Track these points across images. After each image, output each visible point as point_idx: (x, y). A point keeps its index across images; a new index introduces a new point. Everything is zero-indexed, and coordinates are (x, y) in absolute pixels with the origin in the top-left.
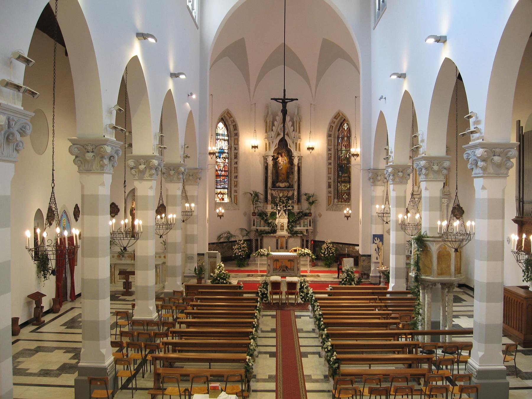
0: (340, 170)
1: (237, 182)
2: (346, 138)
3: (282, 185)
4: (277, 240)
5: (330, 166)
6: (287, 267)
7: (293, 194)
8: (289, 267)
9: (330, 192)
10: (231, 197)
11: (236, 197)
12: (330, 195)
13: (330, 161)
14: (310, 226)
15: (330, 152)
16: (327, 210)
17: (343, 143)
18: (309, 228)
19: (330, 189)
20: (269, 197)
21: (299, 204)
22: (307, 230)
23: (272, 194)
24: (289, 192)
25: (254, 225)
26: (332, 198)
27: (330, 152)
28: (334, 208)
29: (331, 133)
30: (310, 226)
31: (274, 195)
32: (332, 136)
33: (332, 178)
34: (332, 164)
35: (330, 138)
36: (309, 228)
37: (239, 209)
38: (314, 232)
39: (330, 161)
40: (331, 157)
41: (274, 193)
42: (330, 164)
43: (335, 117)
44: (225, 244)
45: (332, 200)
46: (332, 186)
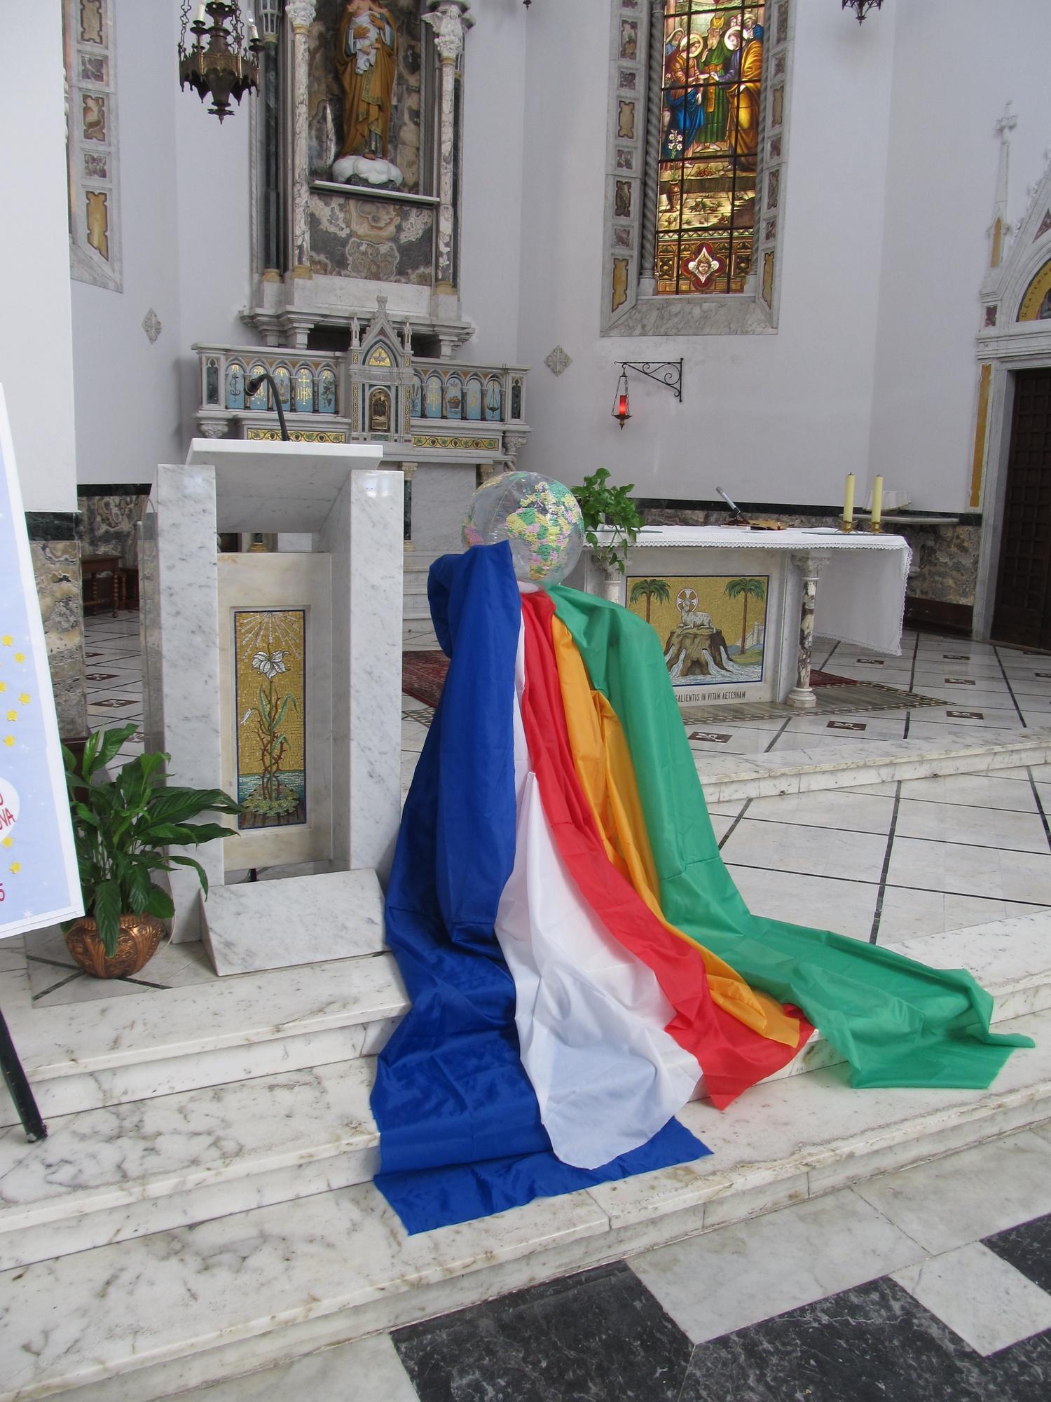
0: (673, 124)
1: (100, 101)
3: (376, 170)
6: (716, 640)
12: (622, 251)
14: (516, 414)
16: (605, 333)
19: (623, 220)
20: (300, 232)
24: (405, 217)
25: (213, 396)
26: (633, 267)
31: (325, 224)
33: (637, 161)
34: (640, 82)
37: (119, 290)
40: (632, 41)
41: (323, 210)
42: (628, 79)
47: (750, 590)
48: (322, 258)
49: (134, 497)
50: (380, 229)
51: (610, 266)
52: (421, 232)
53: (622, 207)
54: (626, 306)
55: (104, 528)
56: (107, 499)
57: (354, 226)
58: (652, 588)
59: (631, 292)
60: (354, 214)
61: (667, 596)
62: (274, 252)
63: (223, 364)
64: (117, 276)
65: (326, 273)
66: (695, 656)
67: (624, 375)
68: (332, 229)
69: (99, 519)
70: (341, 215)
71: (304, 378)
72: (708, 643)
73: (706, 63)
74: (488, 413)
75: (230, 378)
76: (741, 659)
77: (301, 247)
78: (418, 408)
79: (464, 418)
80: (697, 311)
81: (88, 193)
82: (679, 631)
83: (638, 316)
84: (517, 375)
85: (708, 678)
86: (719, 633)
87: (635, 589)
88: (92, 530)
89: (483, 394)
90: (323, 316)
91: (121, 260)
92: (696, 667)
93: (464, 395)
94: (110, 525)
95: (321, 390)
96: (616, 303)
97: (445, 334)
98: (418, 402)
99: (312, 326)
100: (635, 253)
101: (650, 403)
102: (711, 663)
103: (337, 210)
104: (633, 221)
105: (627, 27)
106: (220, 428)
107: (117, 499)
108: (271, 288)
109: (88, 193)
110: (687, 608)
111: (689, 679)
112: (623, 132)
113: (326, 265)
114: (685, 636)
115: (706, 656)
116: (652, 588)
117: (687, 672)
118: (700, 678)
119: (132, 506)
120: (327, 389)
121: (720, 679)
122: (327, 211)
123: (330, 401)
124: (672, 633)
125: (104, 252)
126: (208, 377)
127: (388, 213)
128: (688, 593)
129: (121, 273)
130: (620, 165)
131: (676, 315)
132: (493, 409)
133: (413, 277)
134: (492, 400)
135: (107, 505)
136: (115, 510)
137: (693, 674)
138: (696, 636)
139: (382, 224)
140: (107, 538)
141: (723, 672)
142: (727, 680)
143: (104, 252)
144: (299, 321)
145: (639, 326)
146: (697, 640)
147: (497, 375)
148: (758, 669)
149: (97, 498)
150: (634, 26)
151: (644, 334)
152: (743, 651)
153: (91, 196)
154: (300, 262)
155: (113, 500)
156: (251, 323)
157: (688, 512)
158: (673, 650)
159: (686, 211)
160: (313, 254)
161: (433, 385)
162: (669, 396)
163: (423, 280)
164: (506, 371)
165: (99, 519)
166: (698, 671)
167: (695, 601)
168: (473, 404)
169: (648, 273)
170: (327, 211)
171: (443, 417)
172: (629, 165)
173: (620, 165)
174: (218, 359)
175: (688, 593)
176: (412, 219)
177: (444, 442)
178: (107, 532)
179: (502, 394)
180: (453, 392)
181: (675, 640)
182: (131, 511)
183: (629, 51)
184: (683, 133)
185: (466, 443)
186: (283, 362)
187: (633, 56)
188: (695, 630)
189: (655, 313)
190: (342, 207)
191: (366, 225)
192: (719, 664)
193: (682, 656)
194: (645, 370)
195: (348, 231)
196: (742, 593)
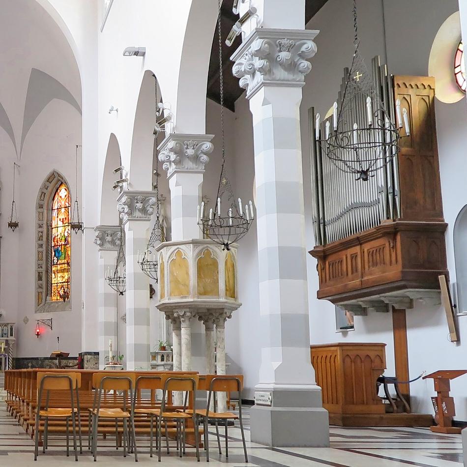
2: (63, 210)
5: (40, 249)
9: (40, 287)
12: (40, 290)
13: (40, 242)
14: (11, 335)
15: (40, 230)
17: (59, 217)
18: (10, 338)
19: (40, 282)
22: (7, 341)
26: (44, 294)
27: (40, 230)
29: (42, 202)
30: (11, 335)
32: (45, 207)
33: (44, 267)
34: (44, 247)
35: (40, 210)
36: (10, 338)
38: (17, 344)
39: (40, 242)
40: (42, 236)
42: (41, 246)
43: (49, 180)
46: (44, 278)
53: (40, 278)
54: (41, 305)
73: (61, 240)
74: (4, 335)
80: (57, 305)
84: (12, 325)
100: (44, 291)
101: (46, 330)
104: (44, 282)
105: (40, 233)
112: (39, 259)
130: (39, 268)
132: (5, 334)
147: (6, 325)
150: (42, 232)
159: (58, 278)
162: (49, 328)
169: (49, 295)
172: (41, 267)
173: (39, 268)
183: (41, 239)
184: (57, 257)
187: (42, 240)
194: (43, 322)
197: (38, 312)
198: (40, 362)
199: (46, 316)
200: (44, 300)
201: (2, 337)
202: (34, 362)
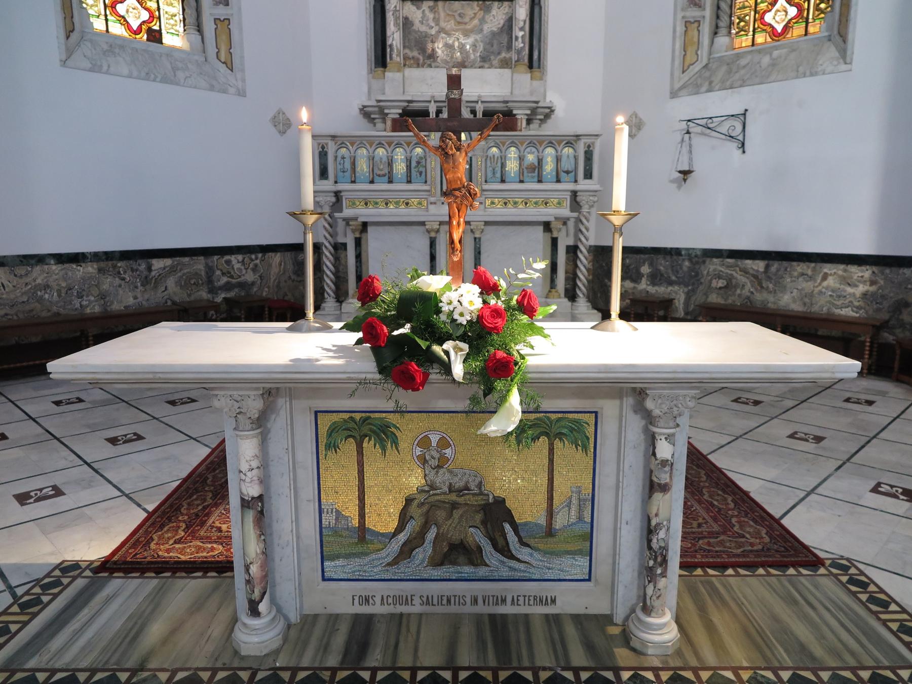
4: (433, 243)
6: (496, 513)
7: (510, 21)
8: (528, 510)
10: (199, 29)
11: (223, 23)
14: (588, 175)
16: (674, 94)
20: (394, 36)
21: (537, 73)
22: (574, 194)
23: (407, 24)
26: (706, 29)
28: (717, 79)
31: (417, 26)
37: (241, 93)
44: (158, 264)
45: (706, 41)
47: (560, 436)
48: (415, 54)
49: (260, 255)
50: (466, 24)
51: (680, 29)
52: (502, 22)
55: (225, 279)
56: (227, 257)
57: (443, 24)
58: (365, 429)
59: (704, 52)
60: (442, 15)
61: (395, 443)
62: (381, 57)
63: (331, 148)
64: (240, 84)
65: (418, 66)
66: (456, 537)
67: (688, 132)
68: (423, 28)
69: (218, 273)
70: (431, 16)
71: (400, 155)
72: (479, 517)
74: (563, 176)
75: (339, 159)
76: (550, 544)
77: (391, 46)
78: (498, 175)
79: (540, 181)
80: (766, 60)
81: (215, 19)
82: (422, 498)
83: (707, 74)
84: (588, 141)
85: (482, 571)
86: (500, 502)
87: (332, 430)
88: (210, 281)
89: (558, 159)
90: (409, 102)
91: (243, 71)
92: (456, 553)
93: (540, 161)
94: (232, 277)
95: (414, 164)
96: (687, 64)
97: (519, 108)
98: (498, 169)
99: (400, 111)
101: (712, 156)
102: (487, 548)
103: (427, 12)
106: (329, 199)
107: (240, 257)
108: (376, 84)
109: (215, 19)
110: (434, 463)
111: (447, 570)
113: (418, 59)
114: (434, 506)
115: (477, 536)
116: (365, 429)
117: (438, 561)
118: (467, 570)
119: (258, 261)
120: (418, 163)
121: (505, 573)
122: (419, 14)
123: (421, 173)
124: (409, 501)
125: (229, 65)
126: (320, 158)
127: (472, 8)
128: (434, 439)
129: (244, 81)
131: (744, 67)
132: (568, 172)
133: (495, 62)
134: (566, 165)
135: (228, 262)
136: (237, 266)
137: (454, 563)
138: (454, 506)
139: (467, 19)
140: (228, 287)
141: (513, 563)
142: (518, 575)
143: (229, 65)
144: (389, 108)
145: (707, 83)
146: (457, 514)
147: (571, 141)
148: (583, 562)
149: (216, 257)
151: (709, 90)
152: (550, 532)
153: (218, 22)
154: (391, 58)
155: (235, 259)
156: (365, 113)
157: (748, 262)
158: (411, 527)
160: (407, 51)
161: (513, 153)
162: (733, 146)
163: (505, 64)
164: (578, 137)
165: (218, 273)
166: (461, 559)
167: (448, 452)
168: (549, 167)
169: (723, 31)
170: (419, 14)
171: (521, 181)
174: (327, 144)
175: (434, 439)
176: (494, 12)
177: (515, 203)
178: (228, 283)
179: (576, 158)
180: (531, 158)
181: (414, 510)
182: (256, 265)
185: (536, 203)
186: (380, 143)
188: (453, 497)
189: (724, 68)
190: (432, 9)
191: (452, 22)
192: (505, 551)
193: (431, 535)
195: (437, 28)
196: (544, 440)
197: (681, 93)
198: (687, 263)
199: (720, 103)
200: (704, 52)
201: (558, 181)
202: (663, 264)
